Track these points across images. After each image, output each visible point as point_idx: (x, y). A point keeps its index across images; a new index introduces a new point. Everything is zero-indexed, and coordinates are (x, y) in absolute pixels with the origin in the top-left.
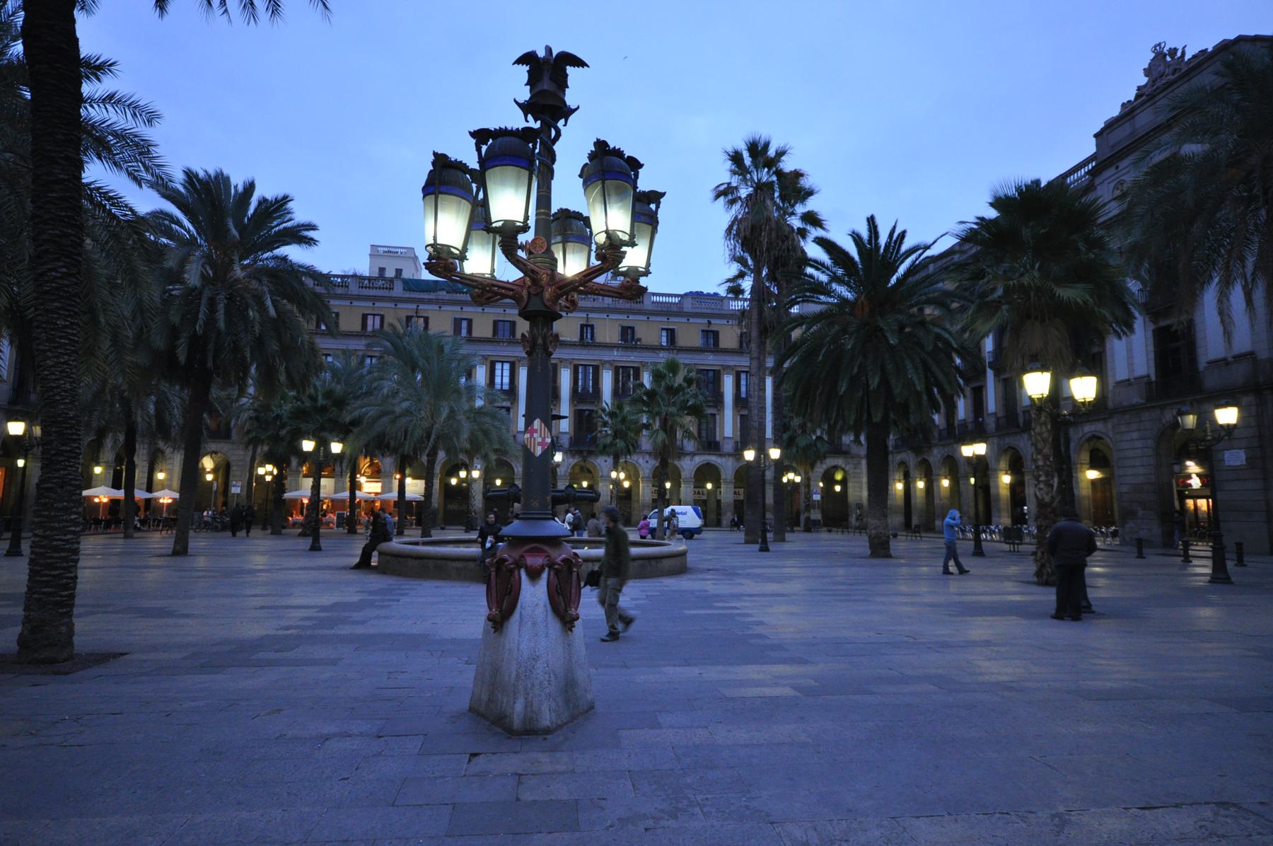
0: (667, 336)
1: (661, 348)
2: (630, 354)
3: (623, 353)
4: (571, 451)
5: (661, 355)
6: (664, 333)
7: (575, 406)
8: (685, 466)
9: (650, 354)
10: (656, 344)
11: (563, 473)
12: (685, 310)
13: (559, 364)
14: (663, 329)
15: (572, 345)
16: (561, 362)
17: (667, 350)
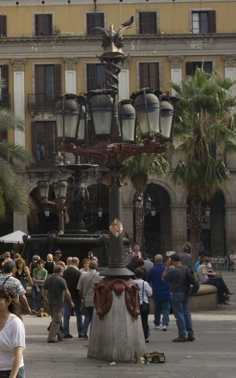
0: (200, 21)
1: (193, 38)
2: (150, 46)
3: (143, 47)
5: (193, 46)
6: (196, 17)
8: (229, 188)
9: (180, 46)
10: (185, 32)
13: (63, 65)
14: (193, 12)
15: (78, 40)
16: (64, 62)
17: (201, 38)
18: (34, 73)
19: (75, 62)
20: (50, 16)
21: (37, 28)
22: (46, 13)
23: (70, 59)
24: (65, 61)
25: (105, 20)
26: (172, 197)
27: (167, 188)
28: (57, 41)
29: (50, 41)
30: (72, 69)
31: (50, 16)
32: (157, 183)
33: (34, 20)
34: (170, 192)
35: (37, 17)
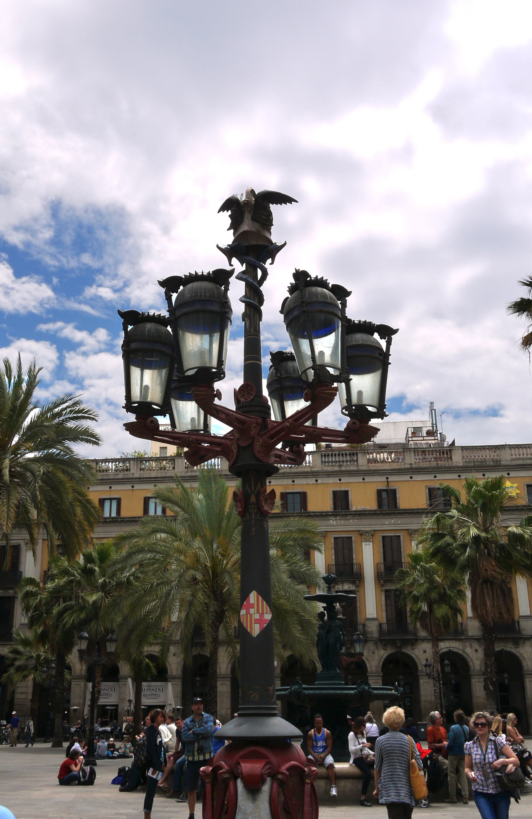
4: (381, 641)
7: (382, 586)
8: (525, 656)
11: (374, 669)
12: (503, 463)
18: (333, 545)
19: (372, 534)
20: (346, 493)
21: (335, 504)
22: (343, 489)
23: (367, 532)
24: (361, 533)
25: (398, 496)
26: (471, 664)
27: (465, 656)
28: (354, 515)
29: (347, 515)
30: (369, 541)
31: (346, 493)
32: (455, 650)
33: (332, 496)
34: (469, 660)
35: (335, 493)
